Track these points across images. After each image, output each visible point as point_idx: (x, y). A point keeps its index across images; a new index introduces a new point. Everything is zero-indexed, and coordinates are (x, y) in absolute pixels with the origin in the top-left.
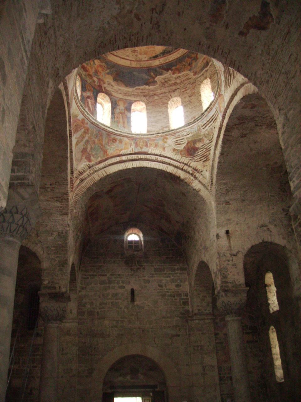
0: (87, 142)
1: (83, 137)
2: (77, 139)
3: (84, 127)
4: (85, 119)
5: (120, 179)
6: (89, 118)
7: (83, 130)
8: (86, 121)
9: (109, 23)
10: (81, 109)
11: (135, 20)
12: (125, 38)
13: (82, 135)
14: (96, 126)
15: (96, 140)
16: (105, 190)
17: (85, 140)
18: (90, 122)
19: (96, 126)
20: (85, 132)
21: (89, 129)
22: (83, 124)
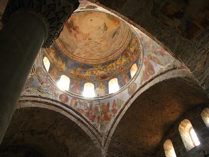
0: (155, 53)
1: (154, 57)
2: (157, 64)
3: (148, 61)
4: (144, 62)
5: (159, 21)
6: (142, 59)
7: (150, 61)
8: (144, 60)
9: (73, 139)
10: (140, 68)
11: (63, 131)
12: (71, 126)
13: (153, 61)
14: (143, 50)
15: (151, 46)
16: (177, 22)
17: (155, 55)
18: (144, 56)
19: (143, 50)
20: (151, 59)
21: (148, 55)
22: (147, 63)
